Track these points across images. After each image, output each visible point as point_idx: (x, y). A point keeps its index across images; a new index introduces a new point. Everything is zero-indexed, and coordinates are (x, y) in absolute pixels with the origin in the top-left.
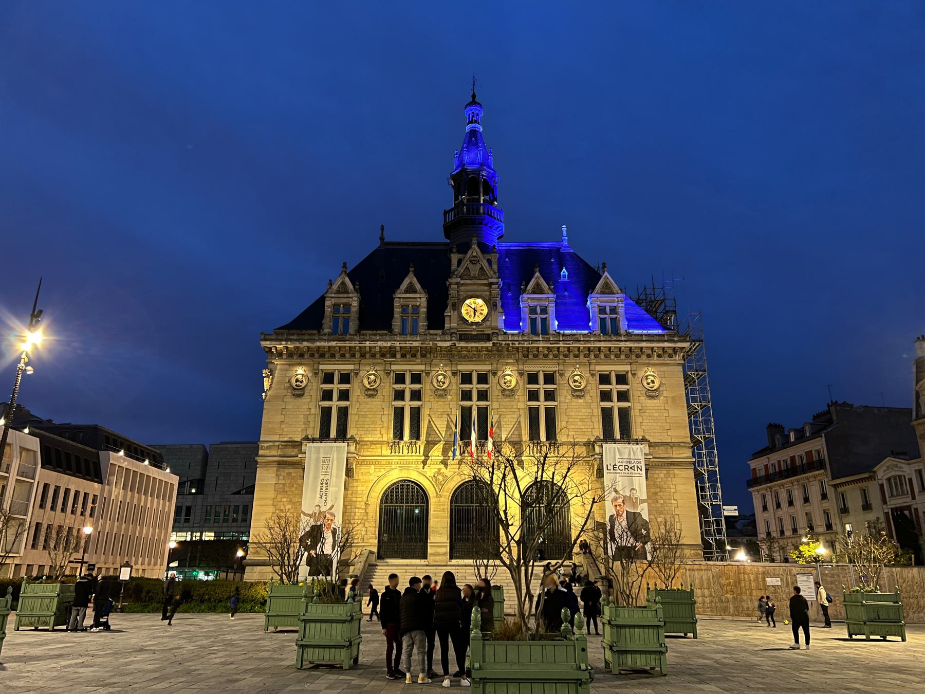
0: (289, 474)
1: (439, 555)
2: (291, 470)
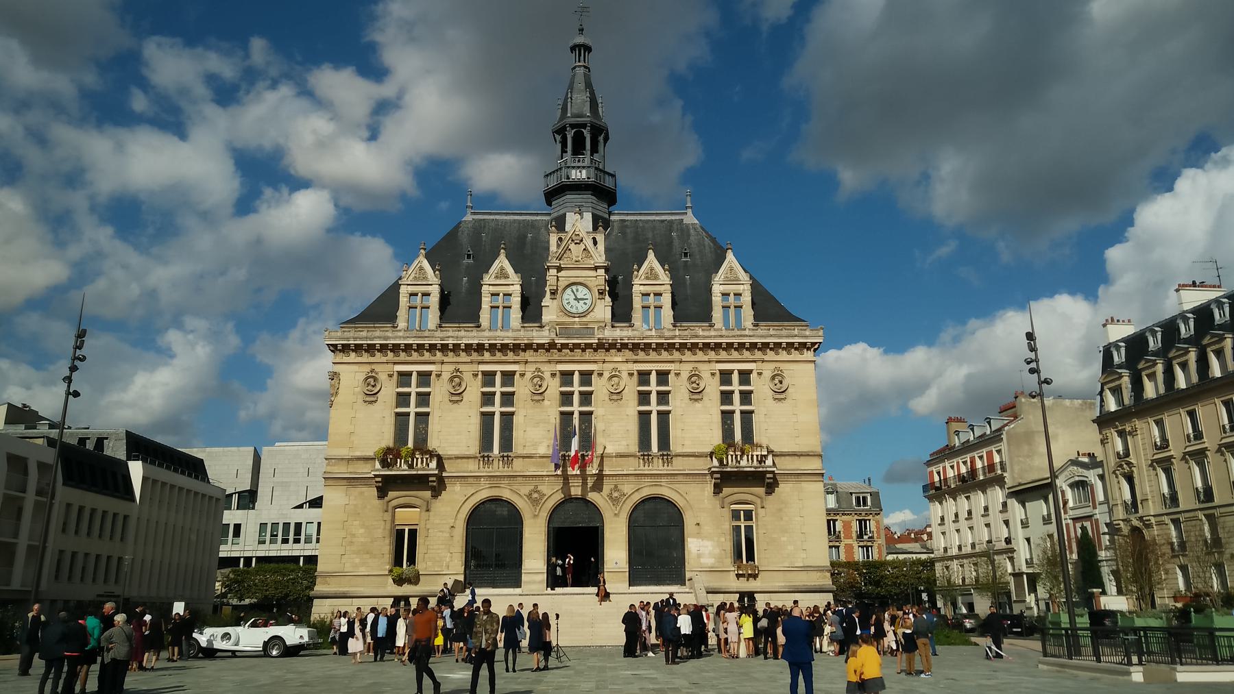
0: (362, 493)
1: (534, 582)
2: (365, 489)
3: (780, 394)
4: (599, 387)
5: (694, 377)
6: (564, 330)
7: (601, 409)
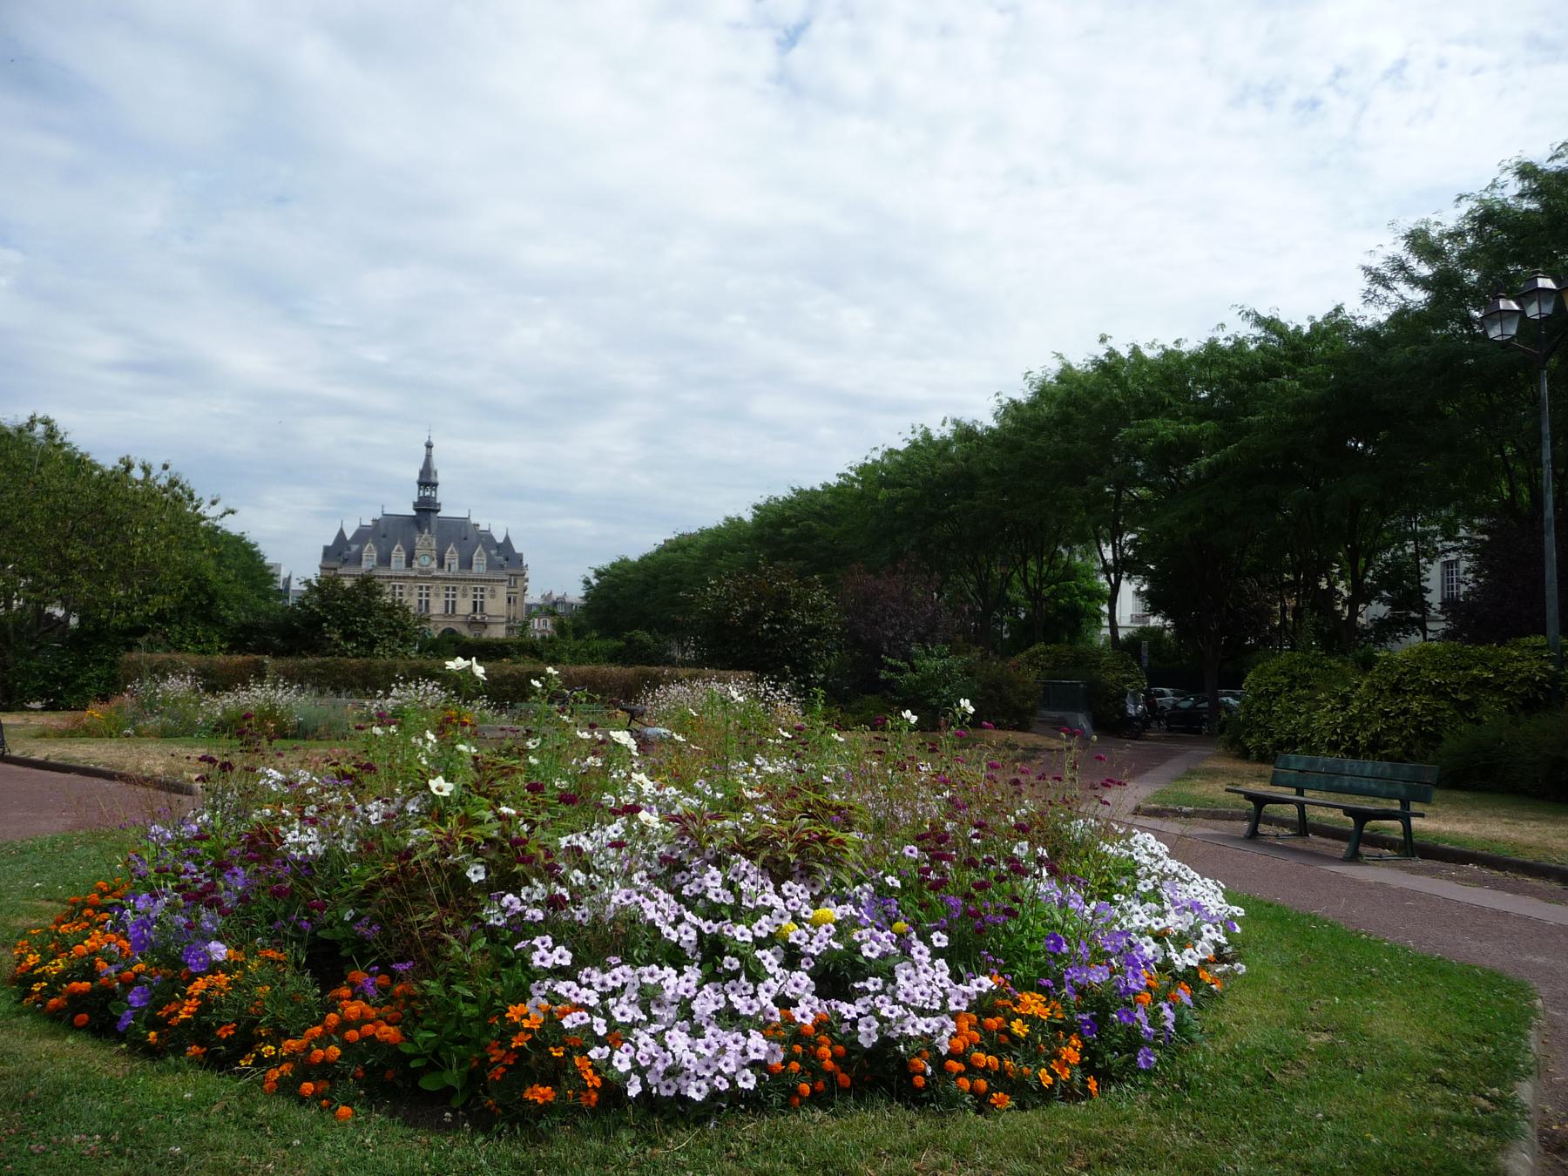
3: (493, 597)
4: (431, 592)
5: (464, 589)
6: (421, 572)
7: (432, 599)
